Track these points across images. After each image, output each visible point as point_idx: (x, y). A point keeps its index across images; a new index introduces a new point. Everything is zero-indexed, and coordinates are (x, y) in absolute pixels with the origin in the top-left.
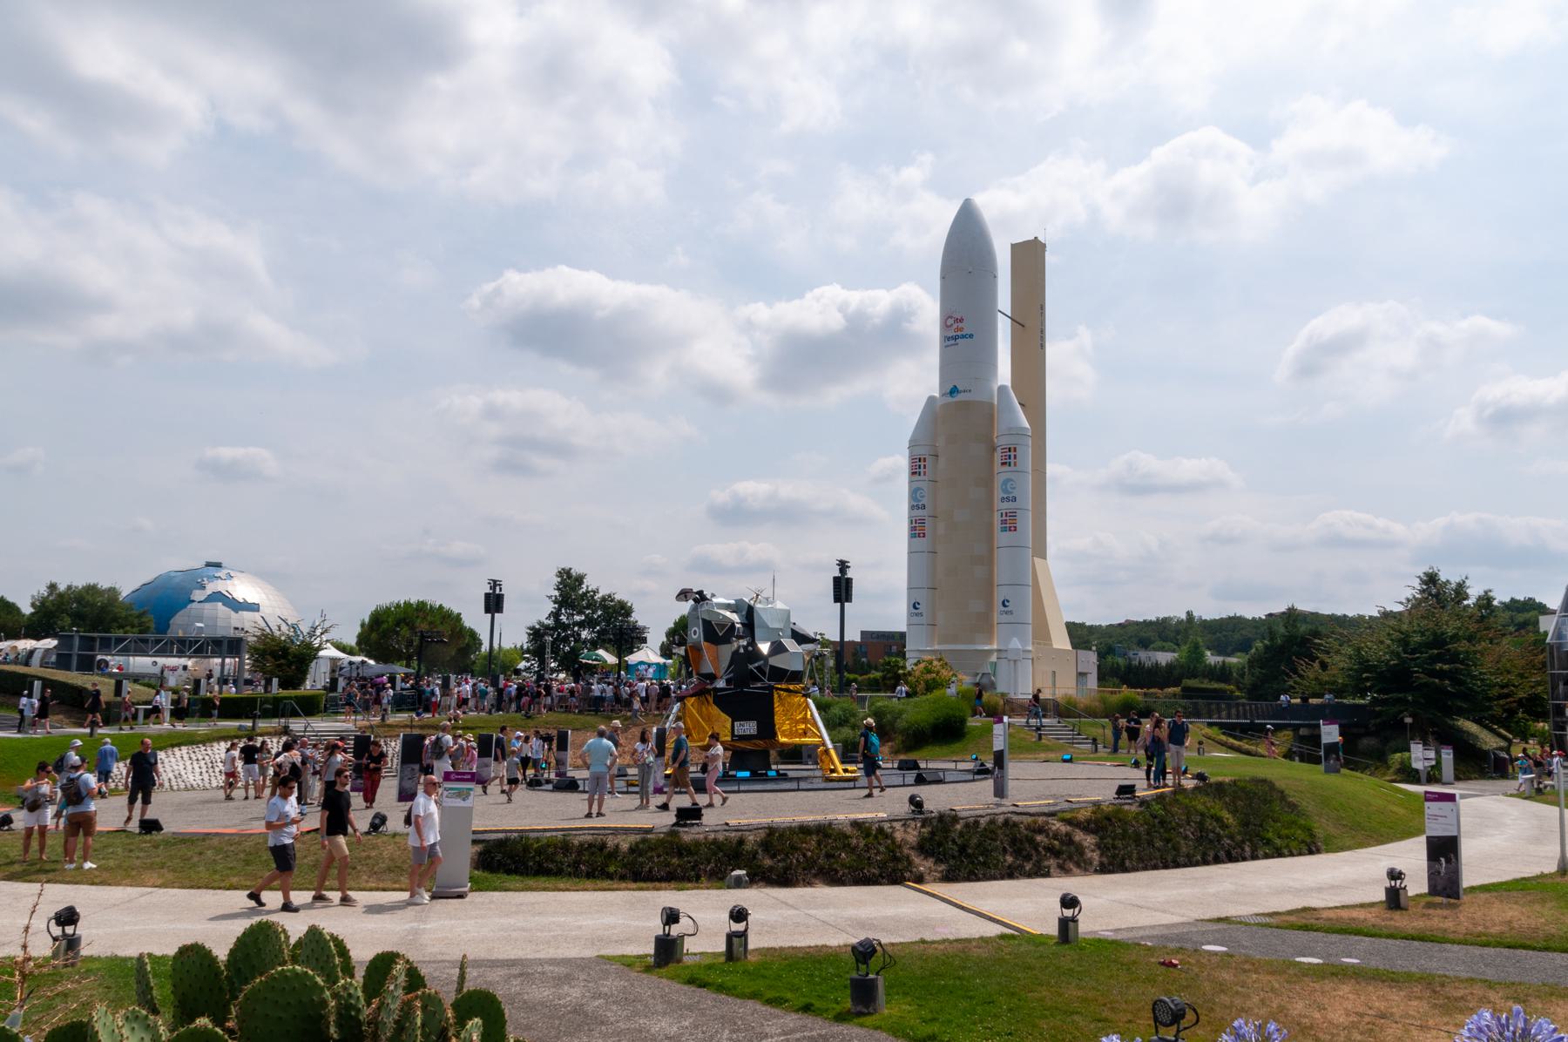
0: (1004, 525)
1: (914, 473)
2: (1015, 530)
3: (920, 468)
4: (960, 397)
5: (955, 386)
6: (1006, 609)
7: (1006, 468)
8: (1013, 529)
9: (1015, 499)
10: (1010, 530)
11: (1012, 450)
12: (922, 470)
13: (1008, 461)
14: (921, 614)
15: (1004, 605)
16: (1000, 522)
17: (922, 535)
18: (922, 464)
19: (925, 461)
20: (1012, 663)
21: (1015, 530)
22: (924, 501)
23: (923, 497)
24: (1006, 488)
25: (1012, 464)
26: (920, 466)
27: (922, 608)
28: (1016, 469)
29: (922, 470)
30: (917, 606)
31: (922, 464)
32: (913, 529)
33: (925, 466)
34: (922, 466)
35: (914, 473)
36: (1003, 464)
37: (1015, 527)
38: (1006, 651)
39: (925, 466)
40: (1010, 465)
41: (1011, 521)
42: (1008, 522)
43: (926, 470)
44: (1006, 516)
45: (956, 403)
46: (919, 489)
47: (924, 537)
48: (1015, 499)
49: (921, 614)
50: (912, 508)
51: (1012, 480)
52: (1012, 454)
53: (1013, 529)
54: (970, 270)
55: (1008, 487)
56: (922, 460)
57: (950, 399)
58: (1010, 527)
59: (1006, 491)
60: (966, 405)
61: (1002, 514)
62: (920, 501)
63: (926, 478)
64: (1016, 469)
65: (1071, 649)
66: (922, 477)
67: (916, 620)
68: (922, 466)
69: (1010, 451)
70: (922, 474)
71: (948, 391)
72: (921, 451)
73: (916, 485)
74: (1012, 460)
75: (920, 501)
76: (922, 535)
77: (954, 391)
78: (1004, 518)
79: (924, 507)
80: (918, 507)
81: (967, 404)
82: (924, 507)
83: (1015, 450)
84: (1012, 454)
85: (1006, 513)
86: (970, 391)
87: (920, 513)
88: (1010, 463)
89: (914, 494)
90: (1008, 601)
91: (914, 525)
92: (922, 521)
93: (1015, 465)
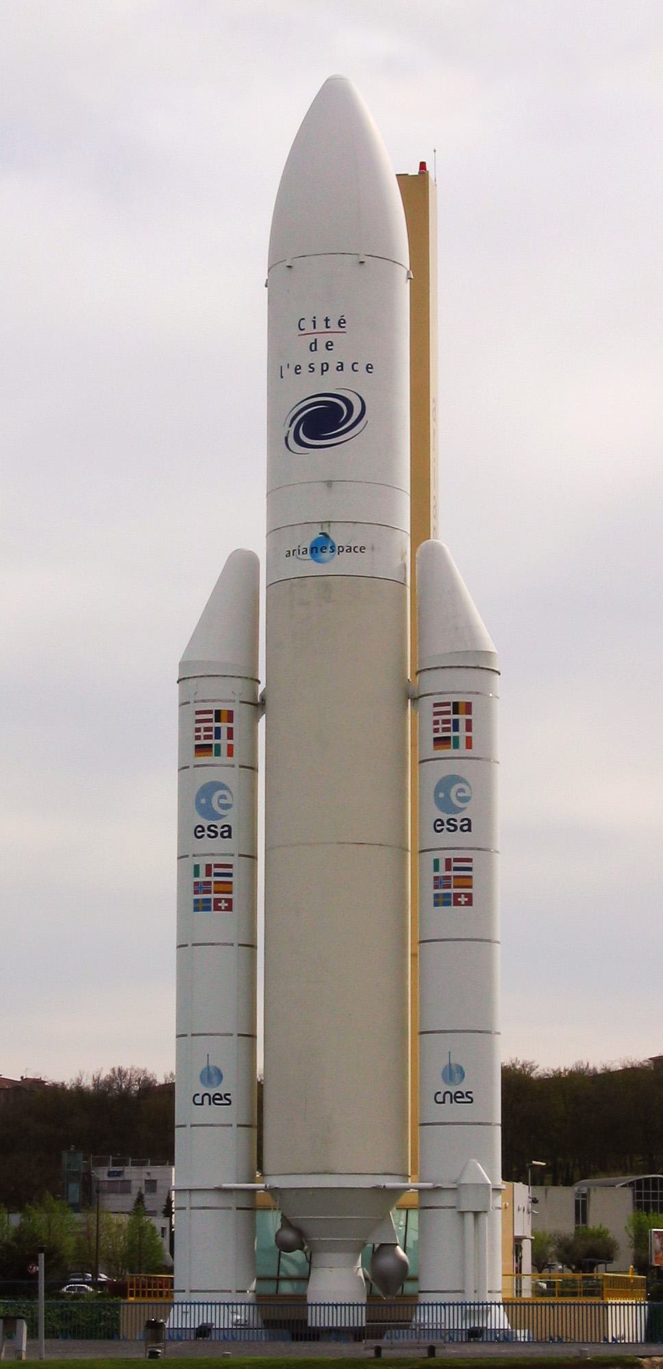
1: (201, 749)
2: (469, 903)
8: (463, 899)
9: (468, 826)
12: (224, 742)
16: (431, 883)
17: (223, 905)
19: (230, 720)
21: (469, 903)
22: (231, 818)
23: (227, 807)
24: (448, 795)
28: (469, 753)
29: (224, 742)
33: (230, 731)
34: (224, 733)
35: (201, 749)
37: (469, 896)
39: (230, 734)
42: (452, 882)
47: (229, 908)
48: (468, 826)
51: (455, 779)
57: (310, 567)
59: (445, 804)
61: (436, 862)
64: (469, 753)
66: (224, 758)
70: (224, 750)
71: (307, 545)
72: (225, 695)
74: (462, 734)
76: (223, 905)
77: (321, 547)
79: (228, 832)
86: (362, 549)
87: (219, 845)
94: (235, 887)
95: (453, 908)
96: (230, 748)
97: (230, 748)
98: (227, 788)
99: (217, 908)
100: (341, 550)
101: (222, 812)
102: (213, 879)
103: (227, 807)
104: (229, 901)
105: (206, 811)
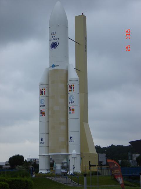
0: (70, 111)
1: (41, 94)
2: (74, 113)
4: (55, 68)
5: (54, 64)
6: (71, 140)
7: (71, 92)
8: (73, 112)
10: (72, 113)
11: (73, 86)
13: (71, 89)
14: (44, 143)
15: (71, 139)
18: (43, 91)
20: (73, 159)
21: (74, 113)
22: (44, 104)
23: (44, 102)
24: (71, 98)
25: (73, 90)
26: (43, 91)
27: (44, 141)
29: (43, 93)
31: (43, 91)
32: (41, 113)
33: (44, 91)
34: (44, 92)
35: (41, 94)
36: (70, 90)
37: (74, 112)
38: (71, 154)
39: (44, 91)
40: (72, 91)
41: (73, 110)
42: (72, 110)
43: (45, 93)
44: (71, 108)
45: (54, 70)
46: (42, 99)
47: (44, 116)
48: (74, 102)
49: (44, 143)
50: (40, 106)
51: (72, 96)
52: (73, 87)
53: (73, 112)
54: (58, 25)
58: (72, 112)
59: (71, 100)
60: (57, 70)
61: (70, 107)
62: (43, 104)
63: (45, 96)
64: (74, 92)
65: (96, 153)
66: (43, 95)
67: (42, 145)
68: (44, 92)
69: (72, 86)
72: (44, 87)
73: (42, 98)
74: (73, 89)
75: (43, 104)
77: (53, 66)
78: (70, 109)
79: (44, 106)
80: (42, 106)
81: (57, 70)
82: (44, 106)
83: (74, 85)
84: (73, 87)
86: (59, 66)
87: (43, 108)
88: (72, 90)
89: (41, 101)
91: (41, 112)
93: (74, 91)
94: (45, 113)
95: (72, 114)
96: (44, 94)
97: (44, 94)
98: (44, 100)
99: (43, 116)
100: (56, 66)
101: (43, 103)
103: (44, 102)
104: (44, 115)
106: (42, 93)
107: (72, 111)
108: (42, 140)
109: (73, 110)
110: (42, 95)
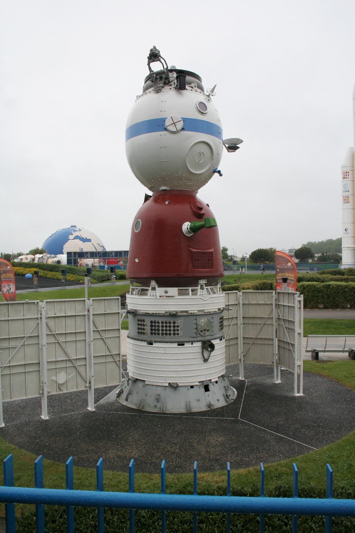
3: (346, 176)
6: (346, 232)
18: (347, 174)
26: (346, 175)
27: (349, 231)
29: (347, 176)
30: (347, 230)
31: (347, 174)
32: (345, 200)
34: (347, 175)
40: (346, 178)
41: (348, 199)
44: (345, 197)
46: (347, 184)
55: (346, 186)
56: (347, 173)
58: (347, 202)
62: (347, 189)
66: (347, 179)
68: (347, 175)
70: (347, 178)
72: (346, 170)
75: (347, 189)
85: (345, 196)
88: (346, 177)
90: (347, 229)
91: (345, 198)
92: (348, 197)
99: (347, 203)
101: (347, 188)
102: (346, 198)
105: (345, 188)
106: (346, 177)
107: (346, 201)
108: (346, 230)
109: (348, 199)
110: (345, 179)
